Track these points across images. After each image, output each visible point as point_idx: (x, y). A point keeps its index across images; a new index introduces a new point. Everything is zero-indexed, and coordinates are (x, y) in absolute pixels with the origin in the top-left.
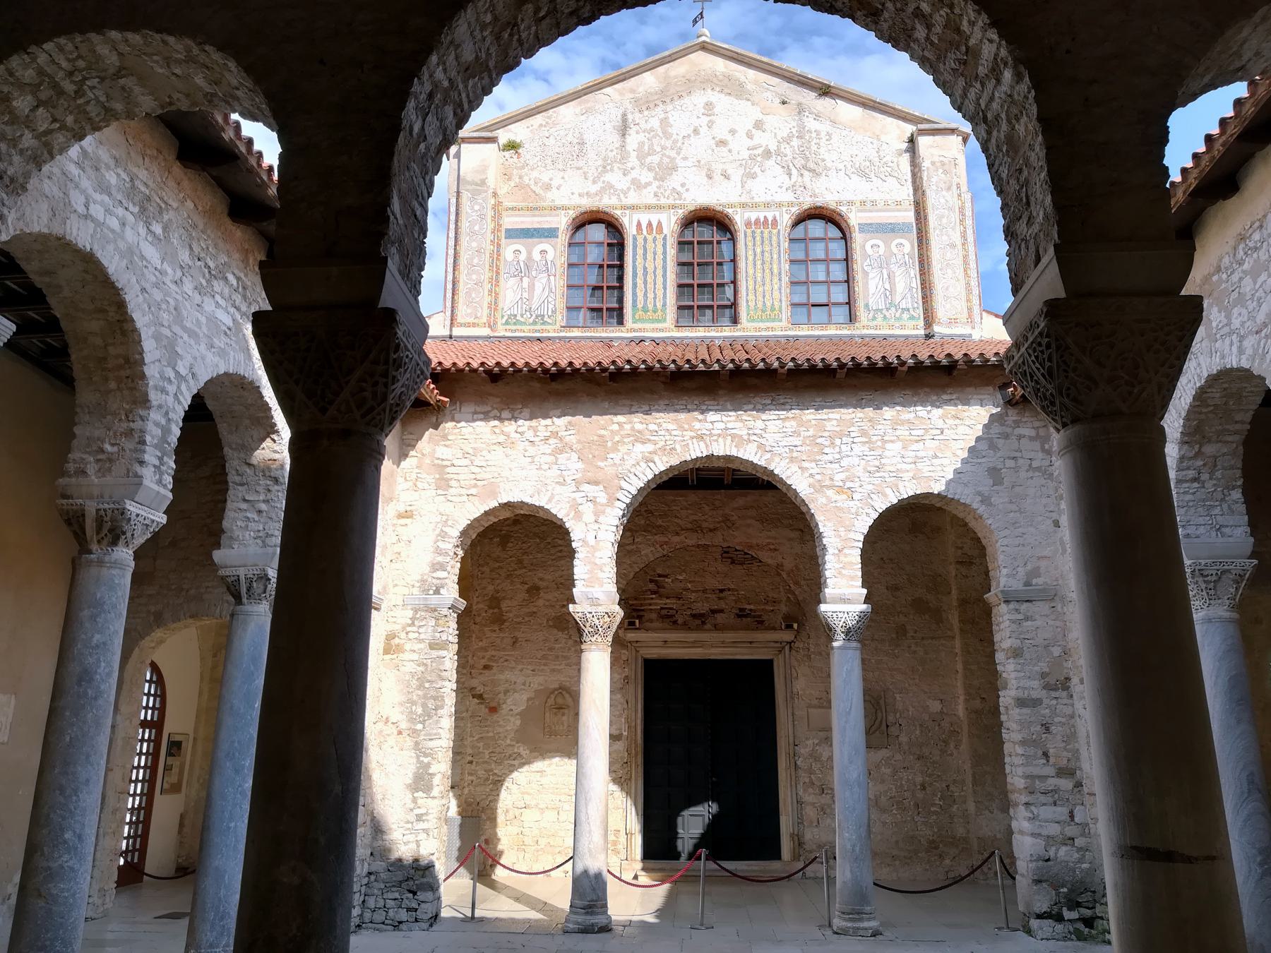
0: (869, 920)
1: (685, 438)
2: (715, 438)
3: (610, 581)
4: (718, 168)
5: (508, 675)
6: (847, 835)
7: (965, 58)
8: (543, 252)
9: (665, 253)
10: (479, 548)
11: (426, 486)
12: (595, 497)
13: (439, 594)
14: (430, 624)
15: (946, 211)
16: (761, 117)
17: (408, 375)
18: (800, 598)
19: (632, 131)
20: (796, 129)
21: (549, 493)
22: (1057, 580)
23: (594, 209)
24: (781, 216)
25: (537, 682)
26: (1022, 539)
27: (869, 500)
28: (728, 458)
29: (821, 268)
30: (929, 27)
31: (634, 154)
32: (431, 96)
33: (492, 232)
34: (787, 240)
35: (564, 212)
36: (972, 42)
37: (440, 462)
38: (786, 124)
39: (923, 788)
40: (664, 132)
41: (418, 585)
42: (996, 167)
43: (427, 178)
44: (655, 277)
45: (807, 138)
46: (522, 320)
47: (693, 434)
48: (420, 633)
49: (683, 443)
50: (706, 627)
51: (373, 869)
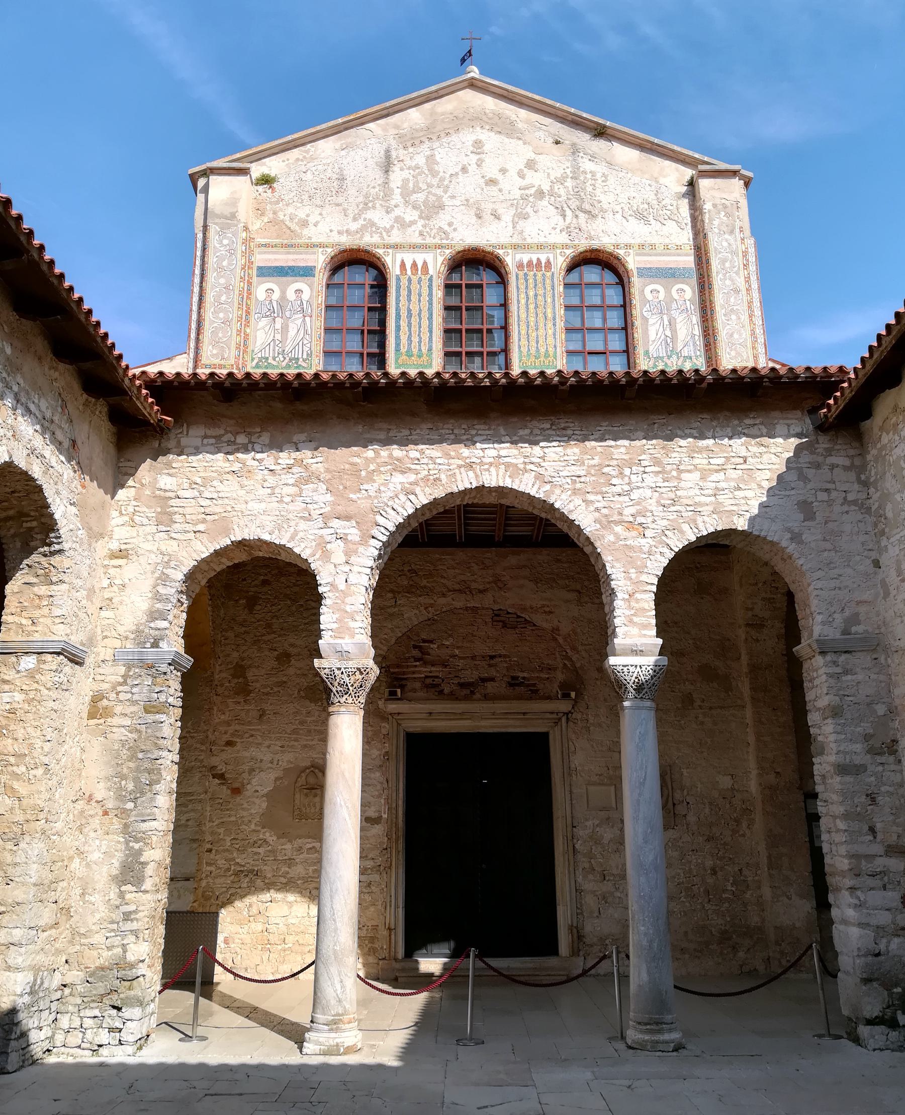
0: (670, 1031)
2: (486, 467)
3: (362, 631)
4: (488, 207)
5: (253, 752)
6: (642, 928)
8: (298, 291)
9: (430, 295)
10: (222, 612)
11: (145, 521)
12: (346, 535)
13: (158, 647)
14: (146, 683)
15: (730, 255)
16: (533, 156)
18: (578, 665)
19: (396, 169)
20: (570, 169)
21: (292, 529)
22: (879, 628)
23: (355, 247)
24: (555, 258)
25: (287, 759)
26: (838, 581)
27: (664, 538)
28: (501, 491)
31: (397, 191)
33: (242, 269)
34: (562, 283)
35: (321, 250)
37: (162, 493)
38: (560, 164)
39: (714, 872)
40: (431, 170)
41: (133, 636)
44: (420, 319)
45: (582, 178)
46: (274, 363)
47: (461, 462)
48: (133, 694)
50: (475, 697)
51: (68, 981)
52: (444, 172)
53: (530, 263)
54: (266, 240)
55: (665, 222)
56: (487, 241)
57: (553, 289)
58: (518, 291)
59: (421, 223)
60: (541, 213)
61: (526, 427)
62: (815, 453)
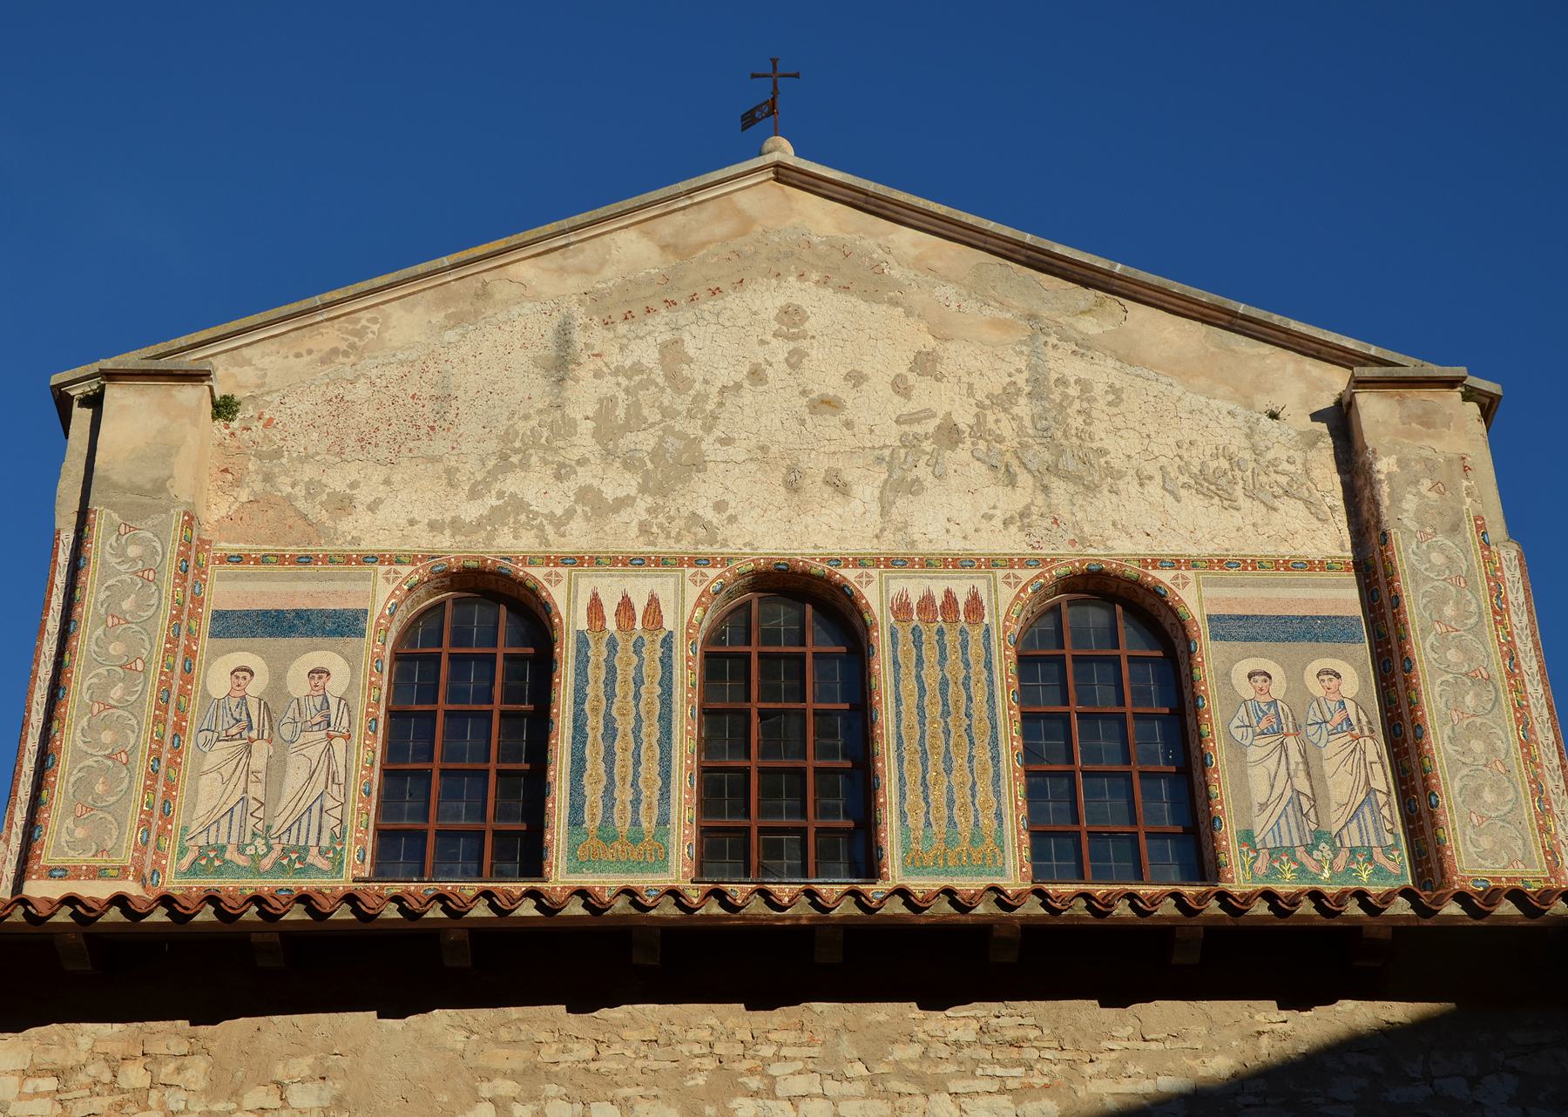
4: (816, 466)
8: (319, 673)
16: (931, 343)
19: (585, 372)
20: (1026, 375)
24: (993, 589)
35: (382, 569)
40: (672, 377)
45: (1056, 397)
46: (241, 861)
52: (706, 382)
53: (927, 602)
54: (242, 545)
55: (1277, 503)
56: (816, 547)
57: (988, 665)
60: (954, 481)
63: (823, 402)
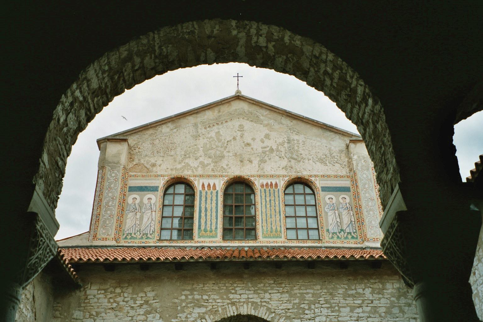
1: (224, 304)
2: (242, 304)
7: (350, 93)
9: (217, 200)
16: (267, 132)
17: (41, 252)
20: (286, 138)
24: (280, 182)
29: (303, 209)
30: (332, 79)
32: (72, 104)
33: (121, 188)
35: (162, 178)
36: (353, 86)
38: (281, 136)
40: (218, 139)
42: (370, 146)
43: (67, 146)
44: (212, 212)
45: (292, 143)
46: (135, 236)
47: (229, 301)
49: (223, 307)
53: (267, 184)
54: (134, 173)
55: (334, 164)
57: (279, 197)
58: (261, 198)
59: (212, 165)
60: (272, 160)
61: (262, 283)
62: (407, 298)
63: (247, 144)
